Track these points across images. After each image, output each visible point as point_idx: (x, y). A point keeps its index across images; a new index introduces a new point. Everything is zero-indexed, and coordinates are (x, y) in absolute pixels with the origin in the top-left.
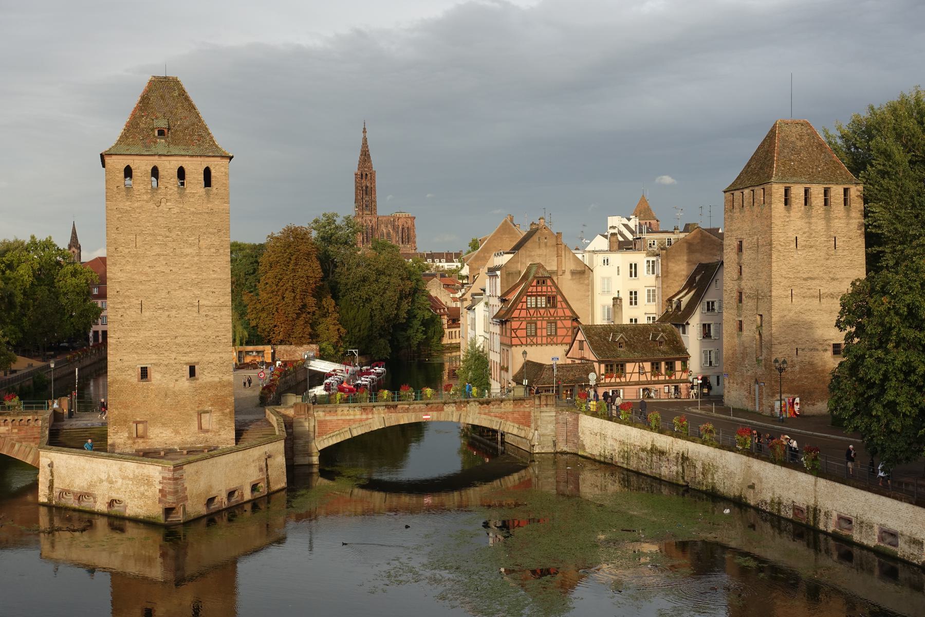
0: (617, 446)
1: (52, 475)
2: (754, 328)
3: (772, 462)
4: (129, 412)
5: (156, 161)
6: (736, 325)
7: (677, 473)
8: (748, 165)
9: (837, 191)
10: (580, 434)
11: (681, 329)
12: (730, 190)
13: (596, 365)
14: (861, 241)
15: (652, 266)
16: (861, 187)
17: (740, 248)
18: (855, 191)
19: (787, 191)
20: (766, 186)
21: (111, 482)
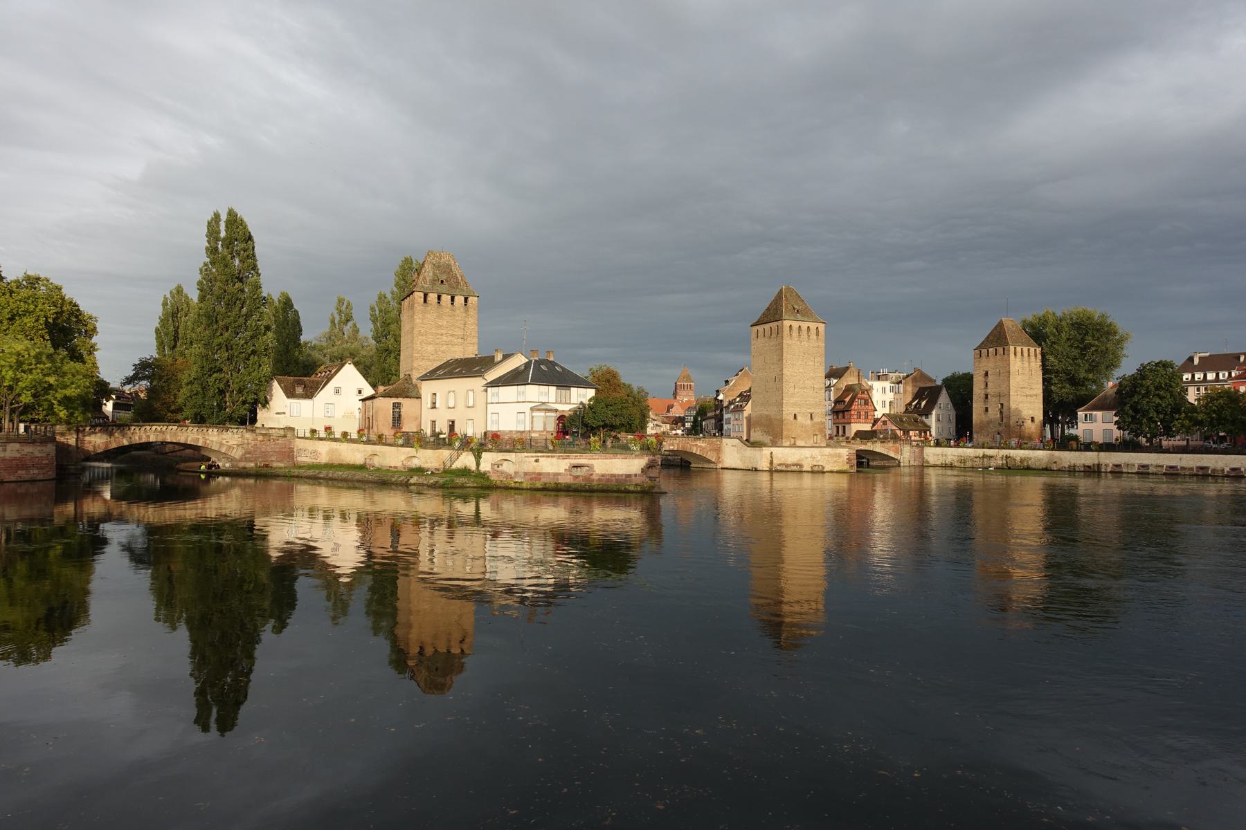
0: (955, 459)
1: (772, 457)
2: (997, 409)
3: (1069, 451)
4: (790, 433)
5: (800, 323)
6: (984, 409)
7: (1002, 464)
8: (988, 337)
9: (1032, 350)
10: (925, 456)
11: (924, 418)
12: (980, 348)
13: (898, 432)
14: (1041, 373)
15: (892, 390)
16: (1040, 349)
17: (986, 374)
18: (1039, 350)
19: (1015, 348)
20: (1006, 347)
21: (813, 458)
